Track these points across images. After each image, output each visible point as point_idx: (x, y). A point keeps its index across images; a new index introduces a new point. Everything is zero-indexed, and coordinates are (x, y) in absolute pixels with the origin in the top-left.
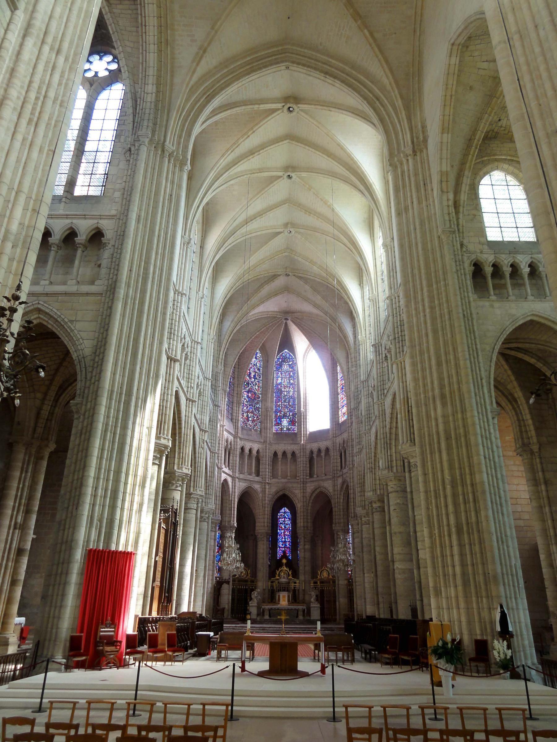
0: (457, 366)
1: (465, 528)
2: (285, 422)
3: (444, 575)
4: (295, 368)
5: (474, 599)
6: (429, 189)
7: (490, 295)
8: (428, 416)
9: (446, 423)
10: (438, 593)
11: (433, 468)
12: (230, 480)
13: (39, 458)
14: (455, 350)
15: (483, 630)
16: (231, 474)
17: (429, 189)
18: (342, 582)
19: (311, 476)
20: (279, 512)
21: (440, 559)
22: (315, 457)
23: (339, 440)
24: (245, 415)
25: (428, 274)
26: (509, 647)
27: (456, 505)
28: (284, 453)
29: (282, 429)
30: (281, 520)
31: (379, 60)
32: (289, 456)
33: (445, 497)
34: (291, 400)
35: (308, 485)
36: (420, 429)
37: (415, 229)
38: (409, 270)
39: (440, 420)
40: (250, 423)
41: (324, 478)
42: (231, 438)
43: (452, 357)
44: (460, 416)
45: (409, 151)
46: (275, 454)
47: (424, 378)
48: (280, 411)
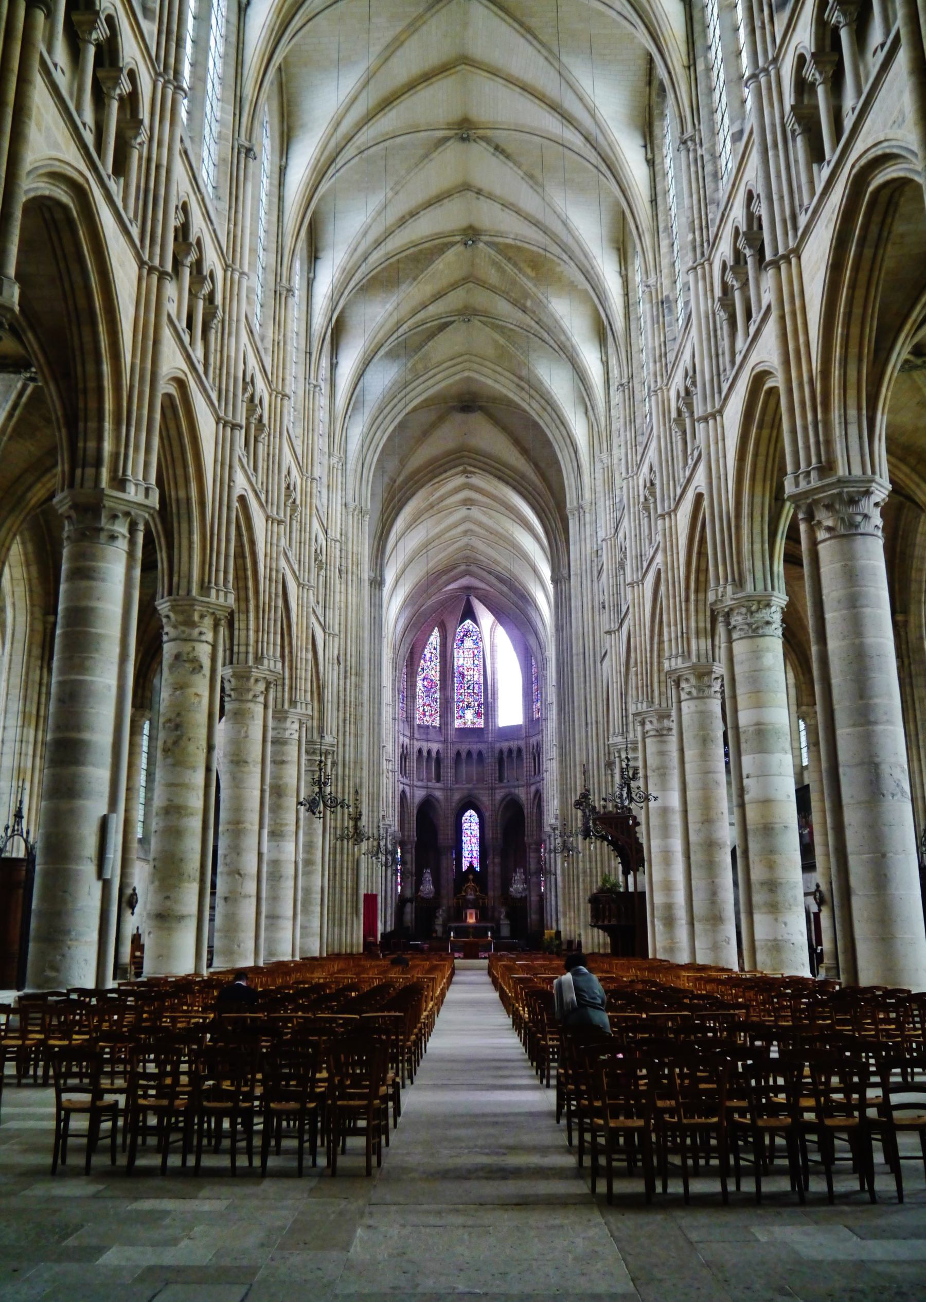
2: (469, 715)
4: (480, 644)
10: (565, 915)
12: (407, 789)
16: (408, 782)
18: (534, 898)
19: (501, 779)
20: (463, 814)
22: (505, 759)
23: (533, 741)
24: (421, 709)
28: (469, 753)
29: (465, 723)
30: (465, 826)
32: (475, 756)
34: (476, 686)
35: (497, 791)
40: (427, 718)
41: (516, 783)
42: (407, 741)
46: (458, 754)
48: (463, 701)
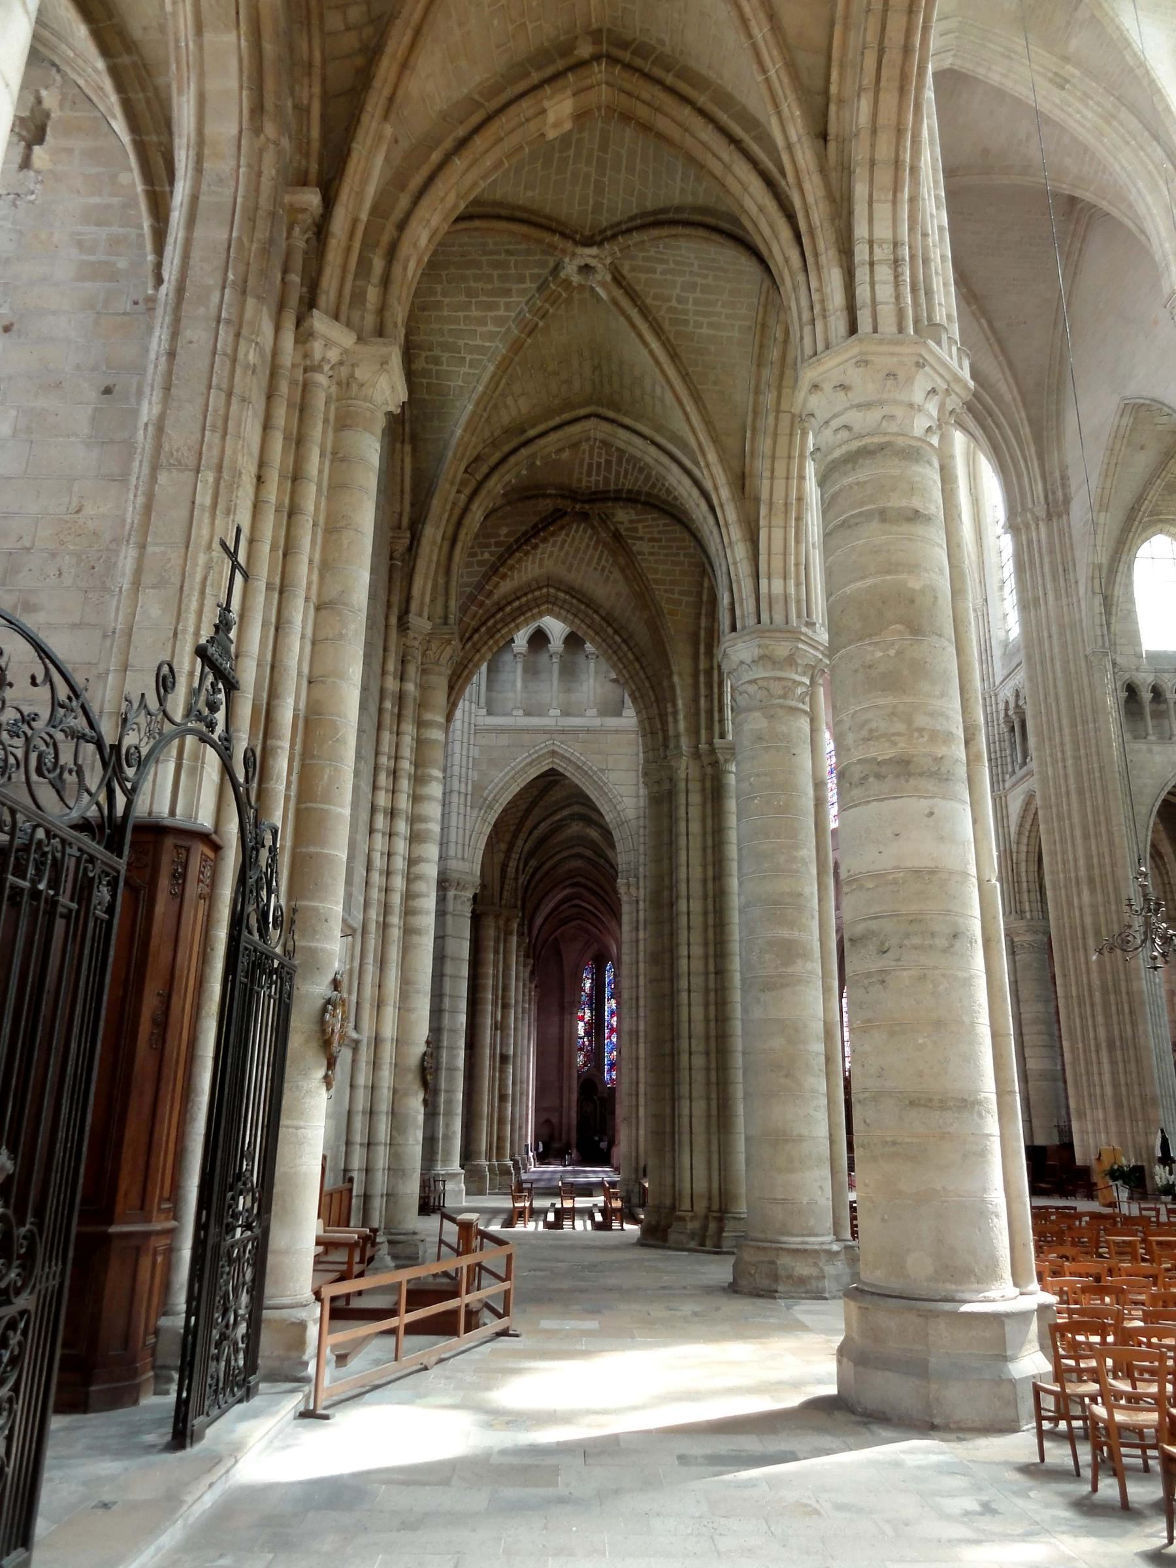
0: (1111, 844)
1: (1118, 1043)
3: (1090, 1096)
5: (1128, 1123)
6: (1073, 581)
7: (1147, 735)
8: (1070, 904)
9: (1095, 914)
11: (1076, 969)
13: (508, 933)
14: (1108, 821)
15: (1138, 1155)
17: (1073, 581)
21: (1084, 1078)
25: (1071, 708)
26: (1171, 1173)
27: (1107, 1016)
31: (999, 363)
33: (1092, 1005)
36: (1058, 919)
37: (1050, 637)
38: (1042, 698)
39: (1087, 911)
43: (1103, 830)
44: (1113, 907)
45: (1041, 512)
47: (1064, 852)
